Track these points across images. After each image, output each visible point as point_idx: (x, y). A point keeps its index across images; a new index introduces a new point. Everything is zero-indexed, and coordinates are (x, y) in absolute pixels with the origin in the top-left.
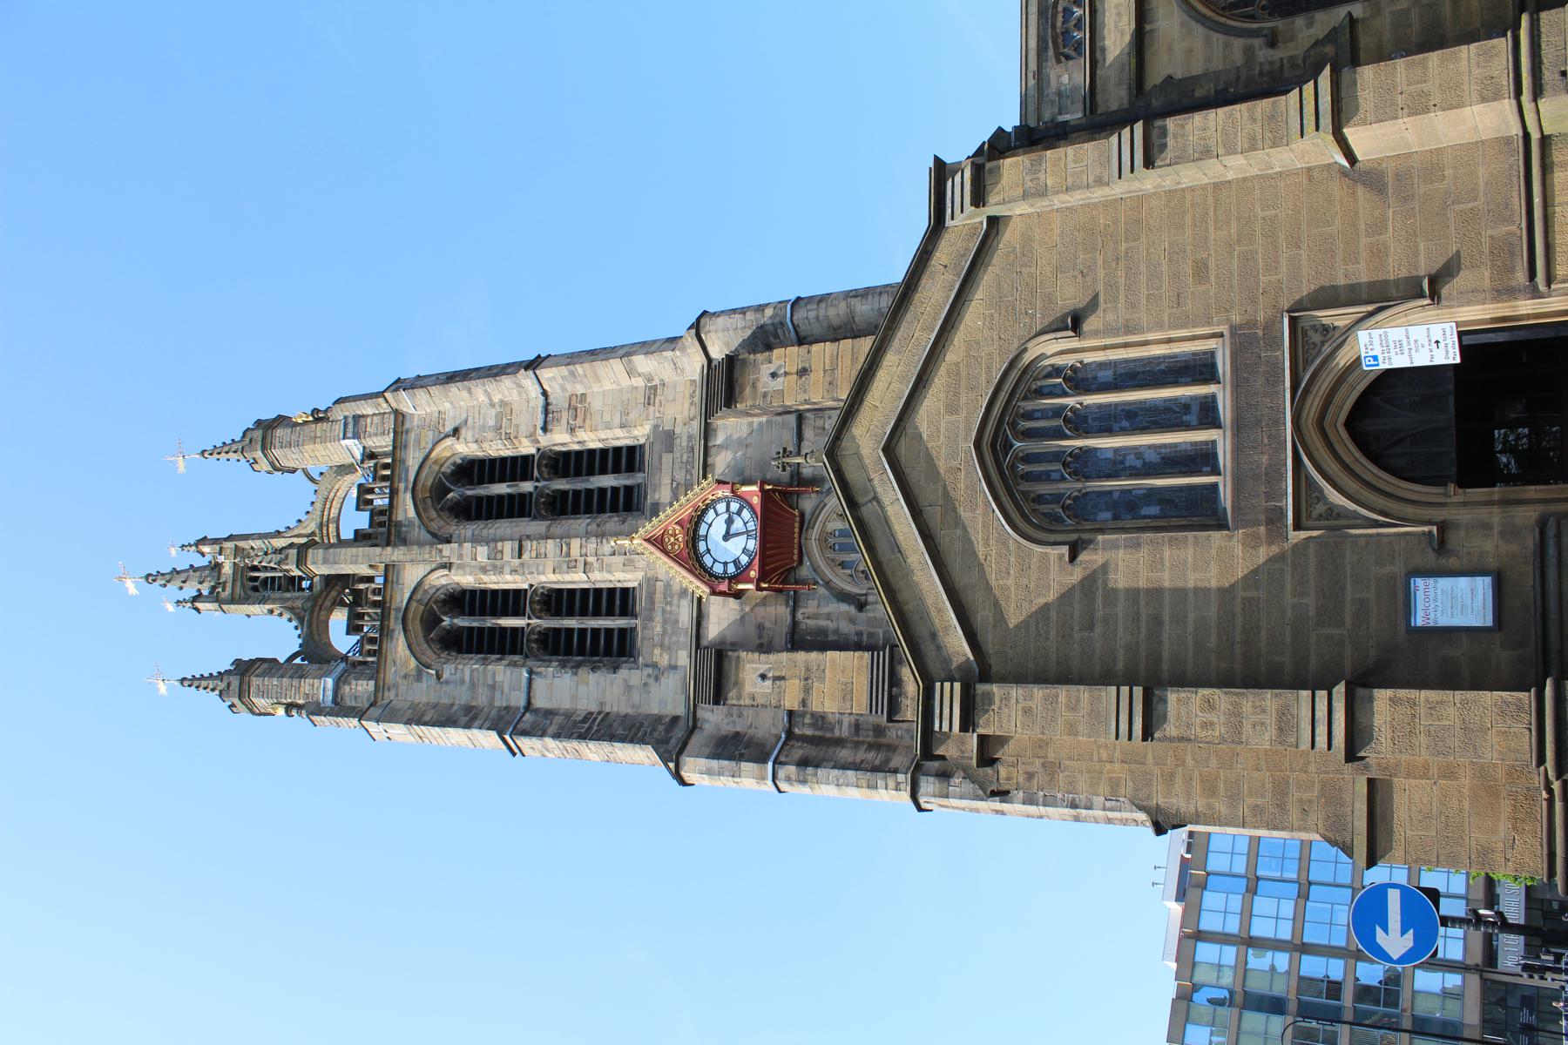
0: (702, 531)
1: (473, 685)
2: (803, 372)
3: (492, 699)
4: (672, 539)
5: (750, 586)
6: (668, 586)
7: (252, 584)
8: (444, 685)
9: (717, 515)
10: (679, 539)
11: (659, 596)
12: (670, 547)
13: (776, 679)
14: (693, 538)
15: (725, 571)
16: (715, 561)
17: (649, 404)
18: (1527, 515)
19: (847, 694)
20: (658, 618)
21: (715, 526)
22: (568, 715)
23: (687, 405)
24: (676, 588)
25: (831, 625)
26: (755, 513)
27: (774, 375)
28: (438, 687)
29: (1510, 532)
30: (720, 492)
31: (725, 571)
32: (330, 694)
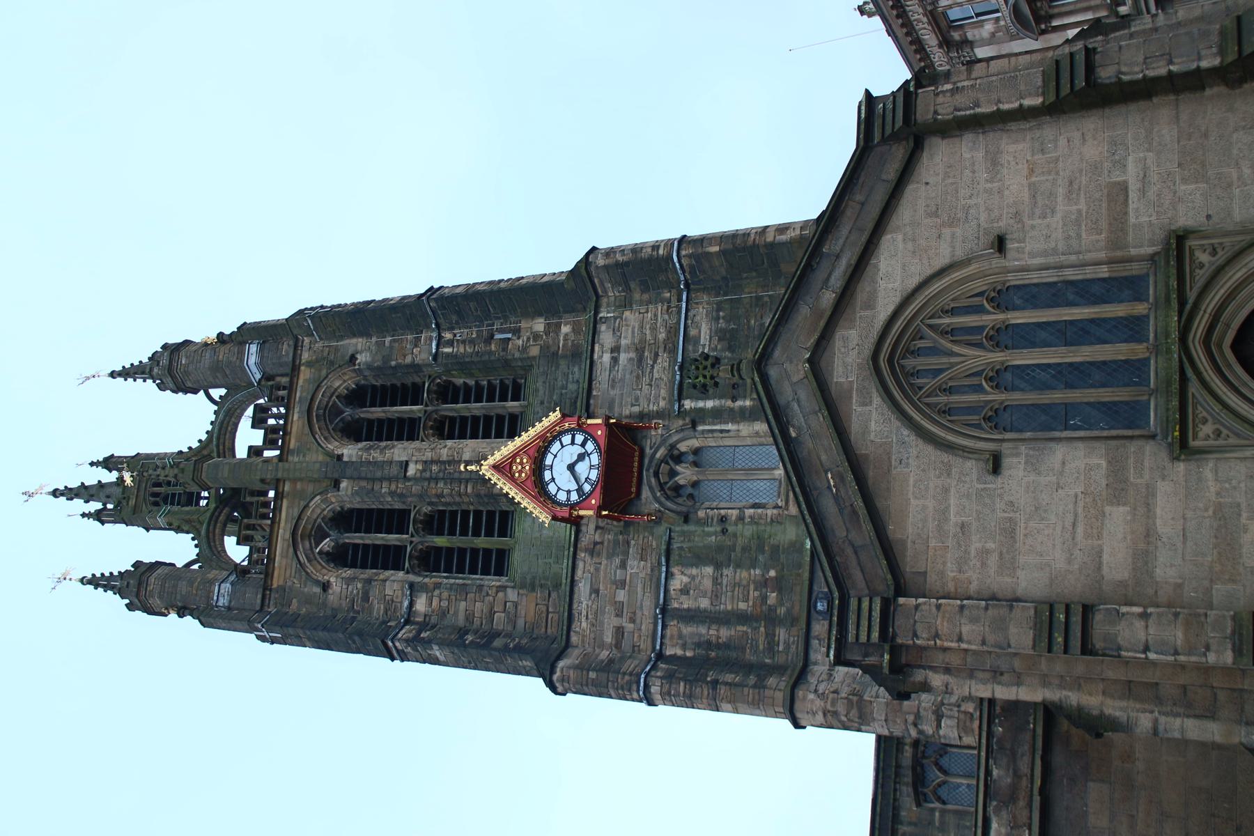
0: (548, 461)
4: (520, 467)
5: (590, 513)
9: (563, 446)
10: (523, 468)
12: (517, 475)
14: (539, 467)
15: (568, 499)
16: (559, 489)
21: (562, 456)
26: (598, 445)
30: (567, 425)
31: (568, 499)
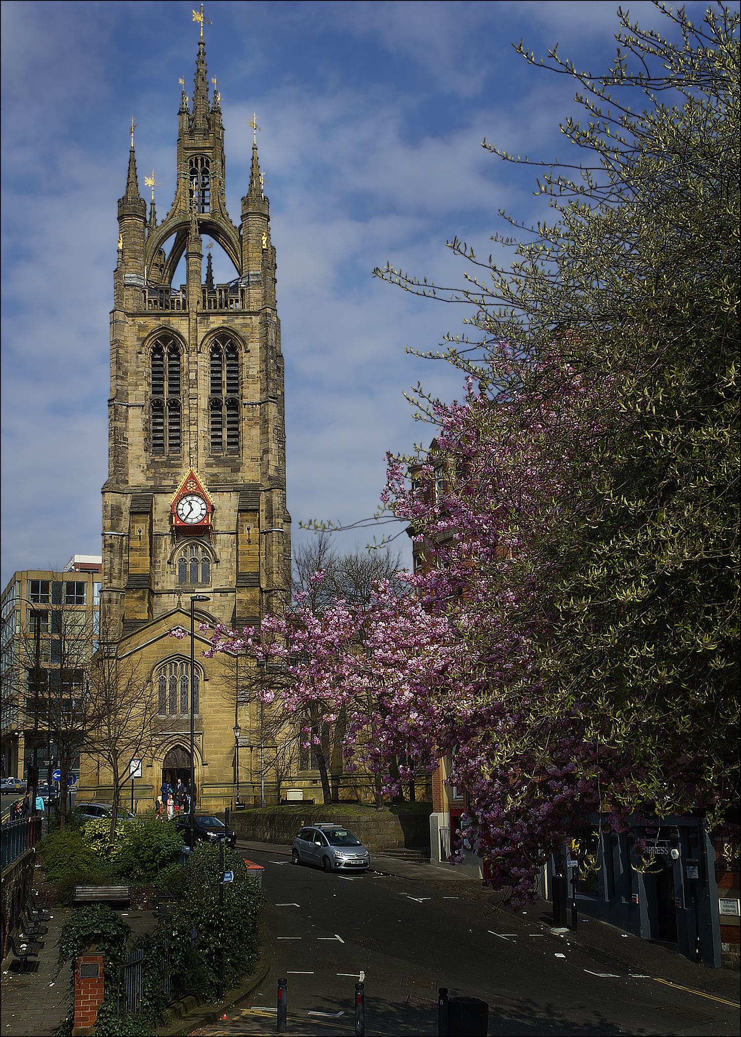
1: (137, 373)
2: (249, 541)
3: (130, 385)
6: (179, 474)
7: (194, 161)
8: (135, 356)
10: (191, 487)
11: (175, 470)
13: (140, 536)
17: (252, 459)
18: (155, 784)
19: (136, 565)
20: (166, 470)
22: (126, 429)
23: (249, 478)
24: (178, 478)
25: (162, 551)
27: (248, 529)
28: (135, 352)
29: (150, 780)
32: (128, 281)
